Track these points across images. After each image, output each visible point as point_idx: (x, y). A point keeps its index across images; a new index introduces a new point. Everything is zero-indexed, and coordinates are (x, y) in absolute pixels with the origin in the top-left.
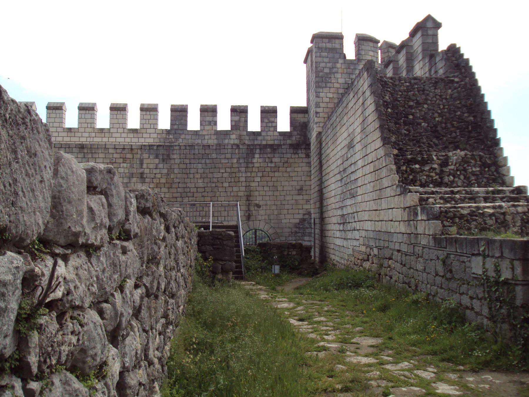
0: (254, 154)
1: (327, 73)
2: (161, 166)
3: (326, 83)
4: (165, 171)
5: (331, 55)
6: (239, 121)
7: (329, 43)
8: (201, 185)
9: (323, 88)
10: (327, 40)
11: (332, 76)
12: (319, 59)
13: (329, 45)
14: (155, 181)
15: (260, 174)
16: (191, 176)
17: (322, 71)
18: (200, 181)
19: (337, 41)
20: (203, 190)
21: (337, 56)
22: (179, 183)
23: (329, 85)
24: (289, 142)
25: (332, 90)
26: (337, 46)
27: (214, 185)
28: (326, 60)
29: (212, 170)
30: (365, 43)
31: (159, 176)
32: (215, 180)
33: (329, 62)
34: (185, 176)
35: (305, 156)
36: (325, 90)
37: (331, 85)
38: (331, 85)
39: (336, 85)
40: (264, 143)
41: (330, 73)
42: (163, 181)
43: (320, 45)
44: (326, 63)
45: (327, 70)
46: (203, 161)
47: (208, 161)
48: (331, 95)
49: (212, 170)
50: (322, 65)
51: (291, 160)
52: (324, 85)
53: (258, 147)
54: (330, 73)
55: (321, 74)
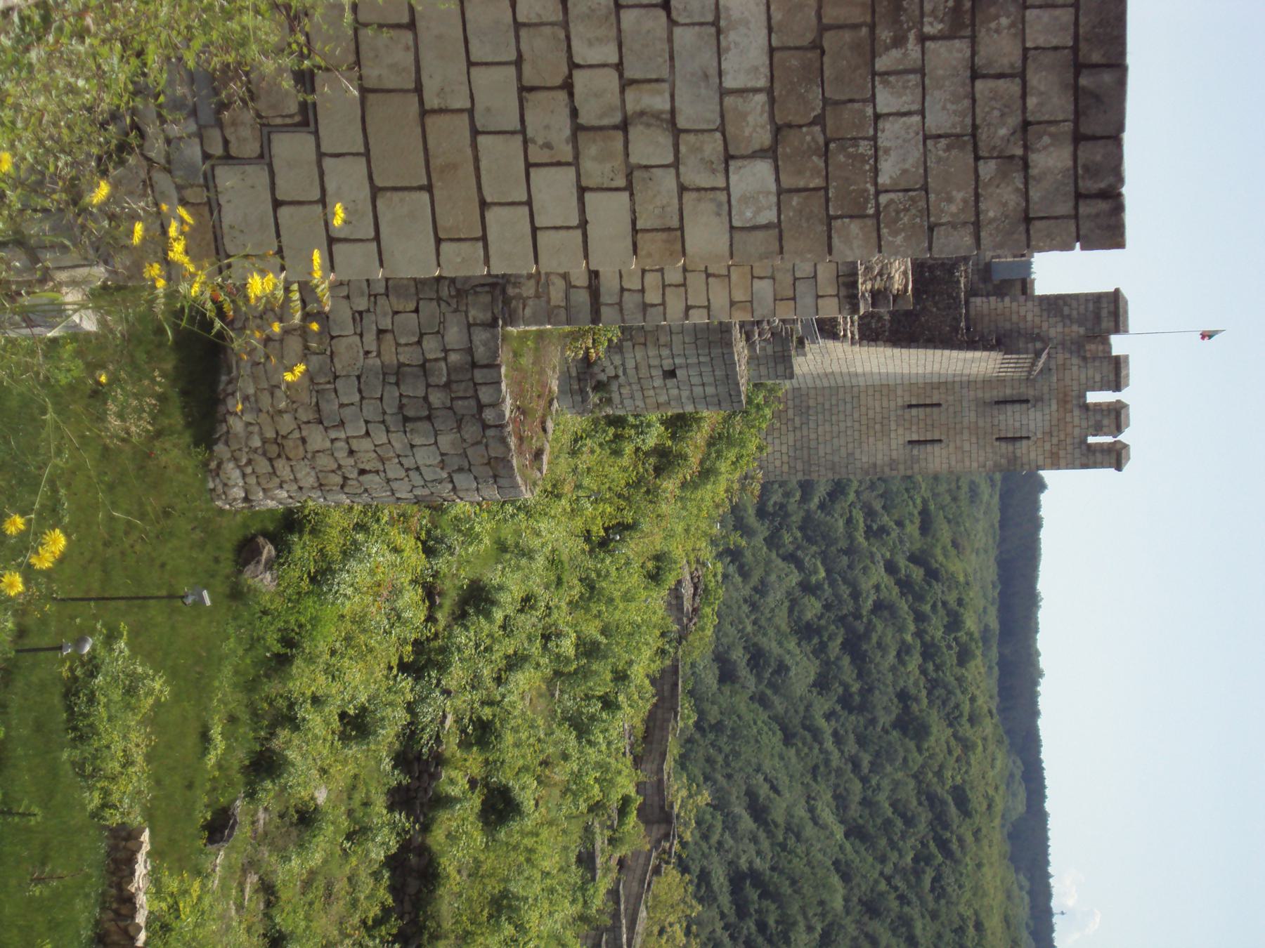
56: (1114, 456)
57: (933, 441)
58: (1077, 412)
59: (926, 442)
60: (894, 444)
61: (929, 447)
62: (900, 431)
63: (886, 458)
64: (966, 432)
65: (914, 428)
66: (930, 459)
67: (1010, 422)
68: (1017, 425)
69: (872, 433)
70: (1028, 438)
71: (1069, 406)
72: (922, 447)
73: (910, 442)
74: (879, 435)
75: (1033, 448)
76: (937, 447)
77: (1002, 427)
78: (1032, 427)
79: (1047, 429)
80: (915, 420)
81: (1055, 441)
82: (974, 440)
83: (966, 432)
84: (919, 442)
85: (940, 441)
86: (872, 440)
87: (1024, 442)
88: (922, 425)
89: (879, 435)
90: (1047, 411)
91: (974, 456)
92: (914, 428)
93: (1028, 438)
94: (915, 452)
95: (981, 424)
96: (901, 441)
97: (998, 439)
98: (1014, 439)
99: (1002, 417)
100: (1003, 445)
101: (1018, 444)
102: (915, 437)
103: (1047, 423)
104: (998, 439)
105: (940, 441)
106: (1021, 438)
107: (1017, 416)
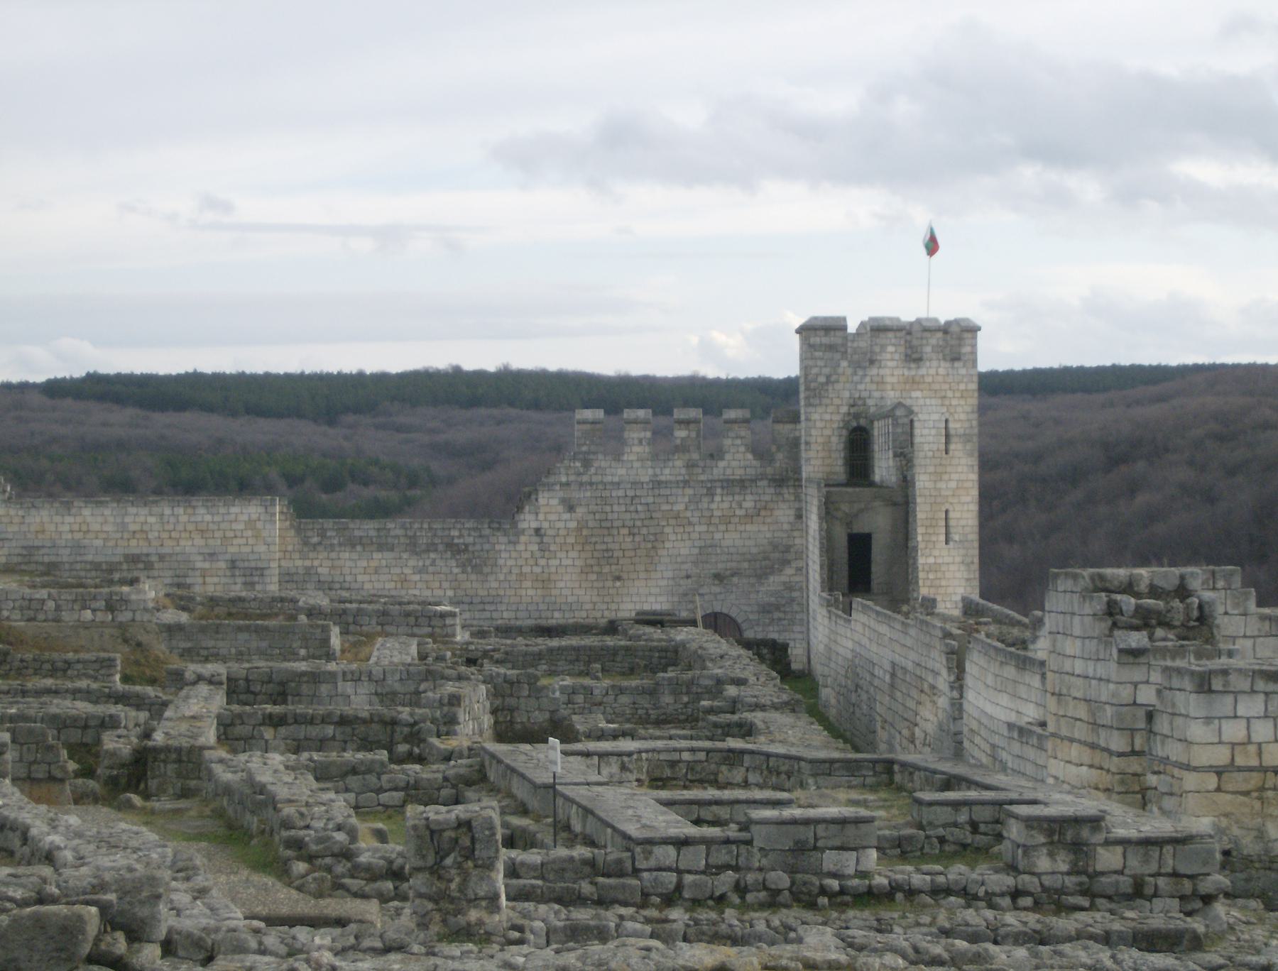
0: (713, 495)
1: (822, 384)
2: (567, 516)
3: (820, 397)
4: (573, 525)
5: (828, 355)
6: (688, 437)
7: (826, 335)
8: (630, 546)
9: (816, 406)
10: (822, 333)
11: (830, 388)
12: (811, 363)
13: (825, 340)
14: (558, 540)
15: (722, 527)
16: (615, 532)
17: (815, 380)
18: (629, 539)
19: (839, 334)
20: (632, 554)
21: (838, 356)
22: (596, 543)
23: (825, 401)
24: (769, 470)
25: (830, 409)
26: (839, 341)
27: (649, 545)
28: (820, 363)
29: (646, 522)
30: (882, 335)
31: (562, 532)
32: (652, 538)
33: (825, 366)
34: (606, 532)
35: (793, 498)
36: (820, 410)
37: (828, 401)
38: (828, 401)
39: (837, 401)
40: (729, 471)
41: (828, 382)
42: (571, 540)
43: (812, 340)
44: (821, 367)
45: (822, 379)
46: (632, 508)
47: (640, 508)
48: (827, 417)
49: (646, 522)
50: (815, 371)
51: (771, 505)
52: (818, 402)
53: (719, 484)
54: (828, 382)
55: (813, 385)
56: (966, 335)
57: (946, 519)
58: (923, 371)
59: (947, 526)
60: (948, 560)
61: (952, 523)
62: (936, 553)
63: (962, 568)
64: (939, 485)
65: (934, 538)
66: (963, 522)
67: (931, 439)
68: (933, 432)
69: (937, 582)
70: (947, 421)
71: (917, 379)
72: (952, 530)
73: (947, 542)
74: (939, 575)
75: (956, 416)
76: (951, 515)
77: (935, 447)
78: (935, 417)
79: (940, 402)
80: (927, 538)
81: (950, 394)
82: (946, 477)
83: (939, 485)
84: (947, 534)
85: (947, 512)
86: (943, 583)
87: (951, 425)
88: (931, 531)
89: (939, 575)
90: (921, 402)
91: (963, 477)
92: (934, 538)
93: (947, 421)
94: (957, 538)
95: (931, 469)
96: (945, 553)
97: (947, 452)
98: (947, 436)
99: (926, 447)
100: (952, 447)
101: (952, 432)
102: (943, 538)
103: (934, 402)
104: (947, 452)
105: (947, 512)
106: (946, 428)
107: (926, 432)
